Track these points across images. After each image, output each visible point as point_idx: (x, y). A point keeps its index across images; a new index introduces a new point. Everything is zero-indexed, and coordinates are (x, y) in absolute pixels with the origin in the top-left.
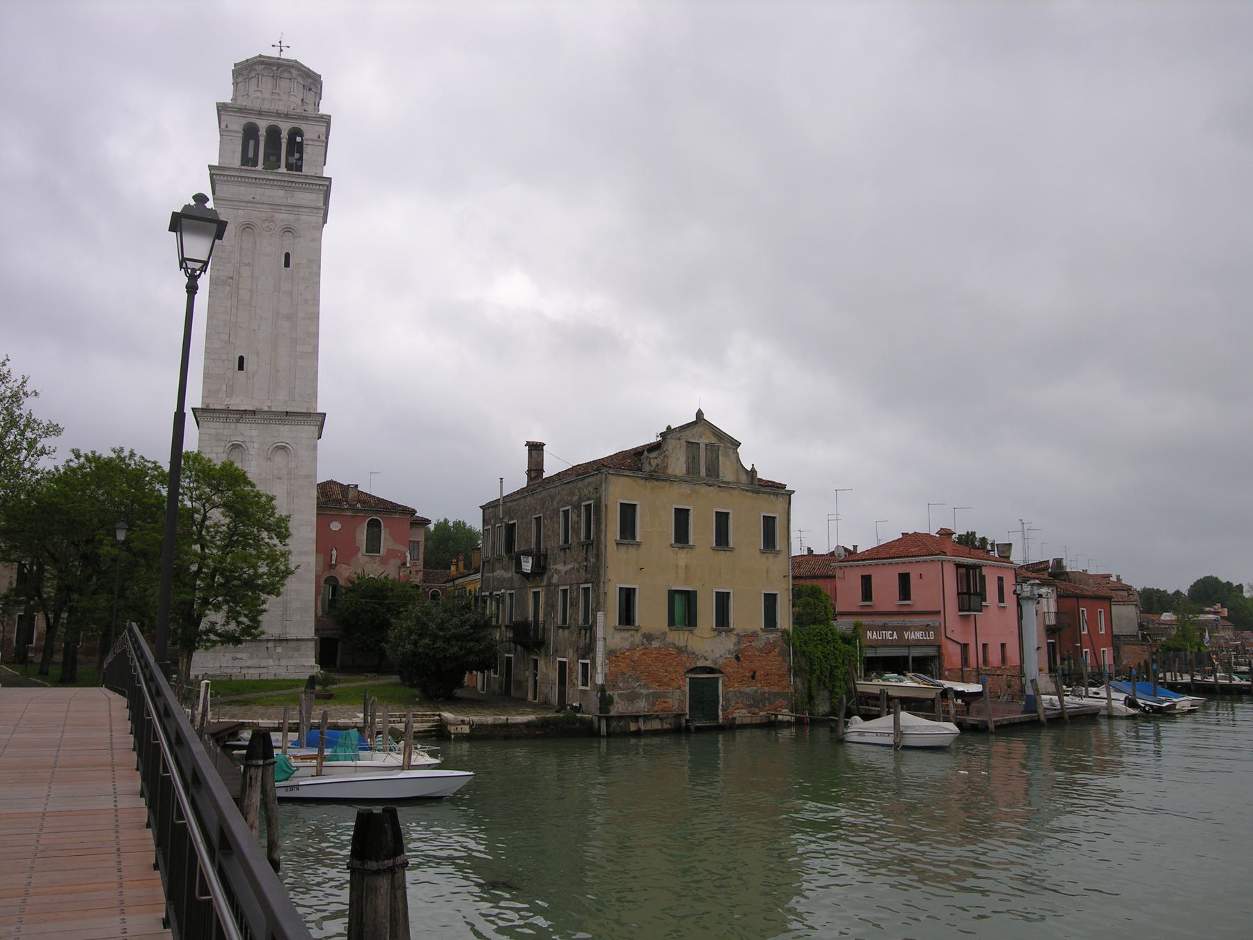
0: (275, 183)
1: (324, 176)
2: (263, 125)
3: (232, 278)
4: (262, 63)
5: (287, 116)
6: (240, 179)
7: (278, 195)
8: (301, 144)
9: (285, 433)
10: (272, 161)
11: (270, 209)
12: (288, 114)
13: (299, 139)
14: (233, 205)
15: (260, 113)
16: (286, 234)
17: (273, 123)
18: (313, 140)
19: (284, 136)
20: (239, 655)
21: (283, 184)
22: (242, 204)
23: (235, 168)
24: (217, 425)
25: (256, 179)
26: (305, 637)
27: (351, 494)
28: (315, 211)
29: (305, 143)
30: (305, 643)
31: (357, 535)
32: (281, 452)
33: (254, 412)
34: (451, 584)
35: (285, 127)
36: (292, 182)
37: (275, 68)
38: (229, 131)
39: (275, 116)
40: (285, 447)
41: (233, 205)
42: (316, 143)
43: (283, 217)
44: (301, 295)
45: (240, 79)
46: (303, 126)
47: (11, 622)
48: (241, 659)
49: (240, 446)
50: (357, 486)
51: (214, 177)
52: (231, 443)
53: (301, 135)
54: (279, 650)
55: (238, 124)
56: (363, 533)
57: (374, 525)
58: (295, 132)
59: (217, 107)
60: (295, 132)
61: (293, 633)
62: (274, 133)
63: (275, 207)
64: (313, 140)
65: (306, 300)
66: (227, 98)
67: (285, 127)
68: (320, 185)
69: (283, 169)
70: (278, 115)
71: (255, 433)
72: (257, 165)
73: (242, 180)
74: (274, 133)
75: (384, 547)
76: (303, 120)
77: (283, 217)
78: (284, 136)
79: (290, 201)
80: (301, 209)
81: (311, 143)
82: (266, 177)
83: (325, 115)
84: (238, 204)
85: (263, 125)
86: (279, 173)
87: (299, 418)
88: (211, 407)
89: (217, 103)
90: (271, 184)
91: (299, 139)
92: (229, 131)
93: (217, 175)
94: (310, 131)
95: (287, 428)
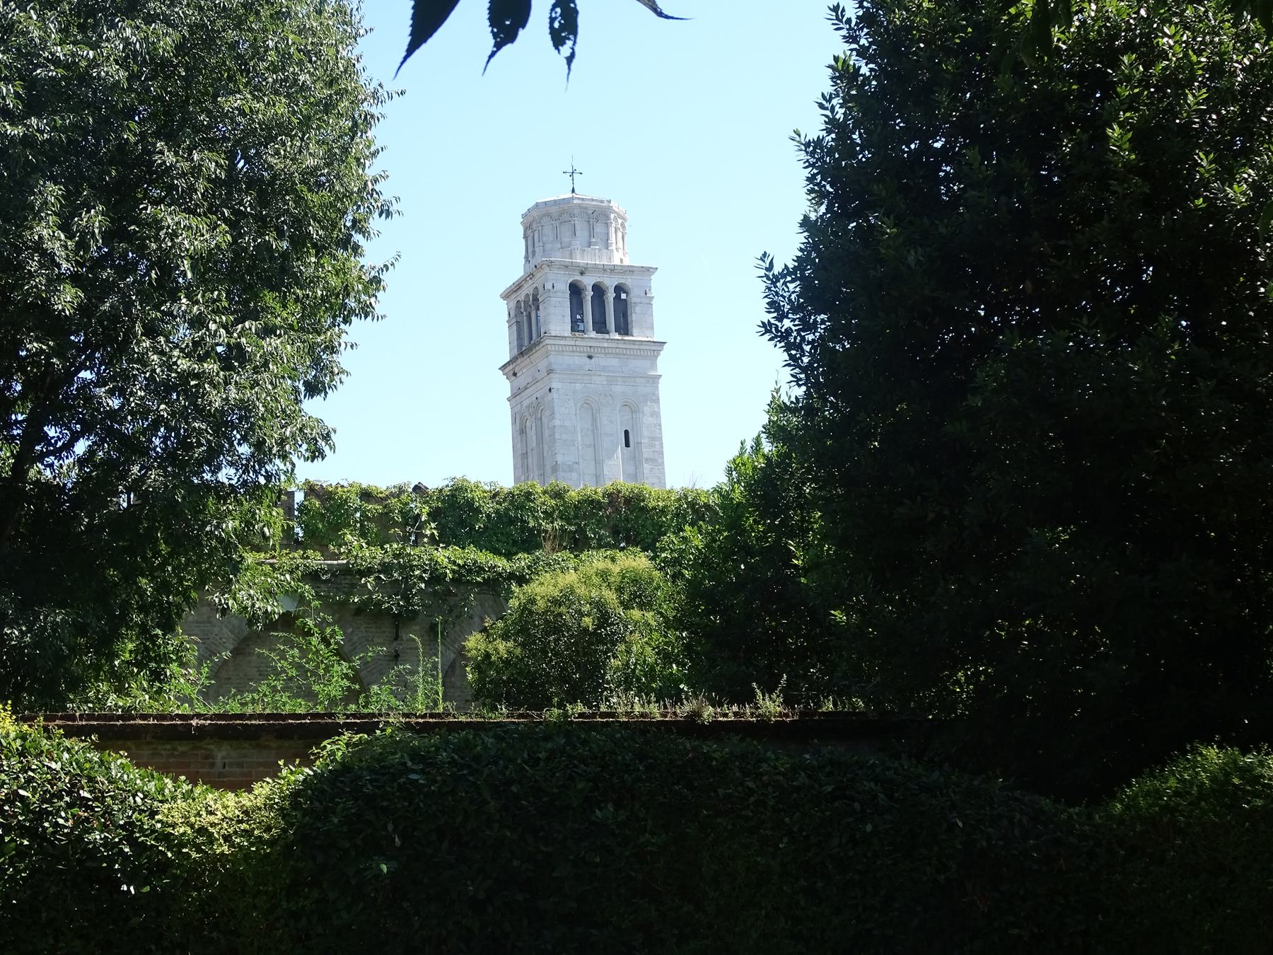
2: (588, 282)
3: (577, 463)
5: (613, 270)
19: (611, 295)
35: (610, 283)
38: (556, 292)
46: (628, 281)
58: (619, 289)
62: (599, 290)
70: (604, 269)
74: (599, 290)
78: (611, 295)
80: (638, 380)
85: (588, 282)
92: (556, 292)
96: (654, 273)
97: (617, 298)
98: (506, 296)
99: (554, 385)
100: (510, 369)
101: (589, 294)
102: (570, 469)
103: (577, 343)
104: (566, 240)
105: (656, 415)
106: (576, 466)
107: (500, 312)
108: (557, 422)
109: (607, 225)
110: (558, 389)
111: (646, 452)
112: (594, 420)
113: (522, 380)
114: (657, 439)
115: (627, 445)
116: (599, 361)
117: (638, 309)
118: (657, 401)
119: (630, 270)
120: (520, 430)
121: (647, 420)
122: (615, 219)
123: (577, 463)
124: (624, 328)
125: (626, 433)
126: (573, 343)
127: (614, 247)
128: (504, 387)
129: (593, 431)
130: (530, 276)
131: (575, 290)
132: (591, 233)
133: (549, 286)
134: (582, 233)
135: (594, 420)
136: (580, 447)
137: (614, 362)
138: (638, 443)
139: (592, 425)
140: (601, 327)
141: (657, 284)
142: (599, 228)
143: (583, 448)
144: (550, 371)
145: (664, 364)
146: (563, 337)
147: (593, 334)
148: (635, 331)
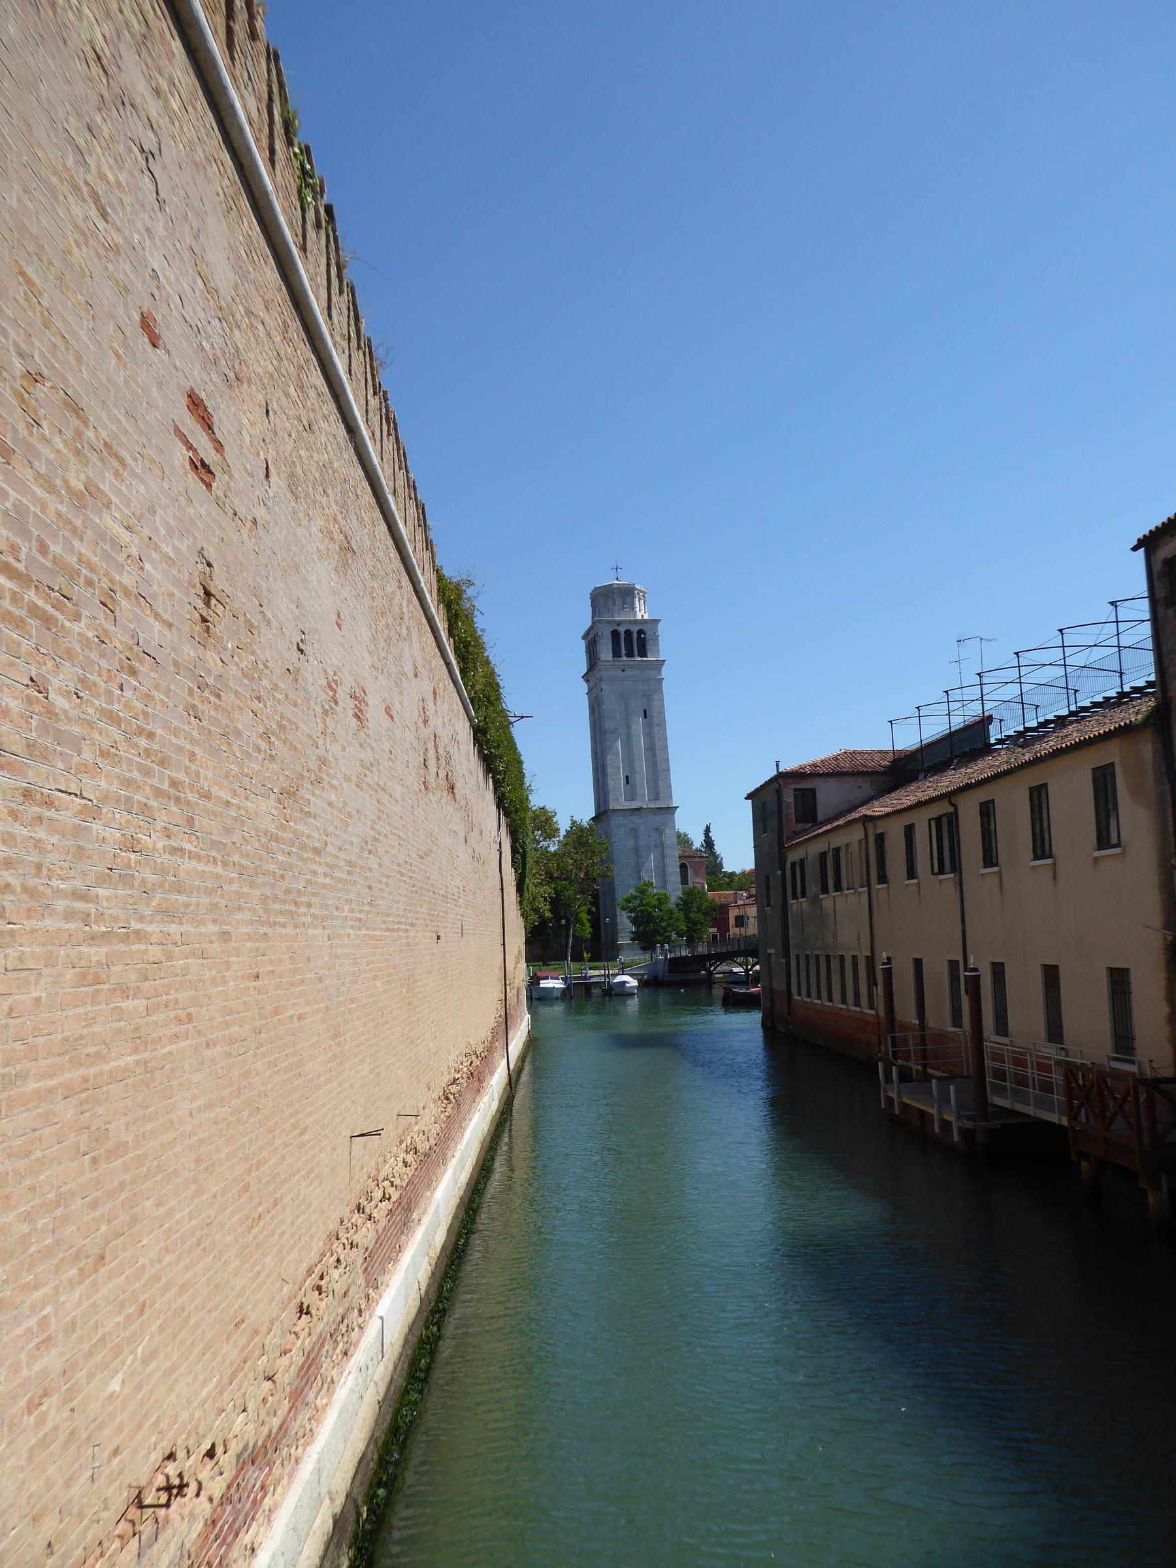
2: (622, 629)
5: (636, 622)
8: (644, 638)
9: (658, 819)
13: (643, 636)
19: (635, 636)
35: (635, 629)
46: (645, 627)
53: (644, 633)
58: (640, 632)
67: (635, 629)
71: (640, 821)
74: (628, 633)
78: (635, 636)
85: (622, 629)
91: (643, 636)
95: (657, 817)
97: (639, 637)
98: (584, 638)
99: (603, 687)
100: (586, 677)
101: (623, 636)
102: (613, 732)
104: (610, 607)
105: (662, 700)
107: (582, 646)
108: (605, 707)
109: (633, 597)
111: (656, 721)
112: (626, 704)
113: (591, 684)
114: (662, 713)
115: (645, 717)
116: (629, 672)
117: (650, 643)
118: (662, 692)
119: (646, 621)
120: (592, 711)
121: (656, 703)
122: (638, 594)
124: (643, 653)
125: (645, 711)
127: (637, 609)
128: (584, 687)
130: (592, 628)
131: (615, 634)
132: (624, 603)
133: (600, 634)
134: (619, 602)
135: (626, 704)
137: (636, 672)
140: (630, 654)
141: (661, 629)
142: (628, 599)
144: (601, 680)
145: (665, 672)
147: (625, 658)
148: (649, 655)
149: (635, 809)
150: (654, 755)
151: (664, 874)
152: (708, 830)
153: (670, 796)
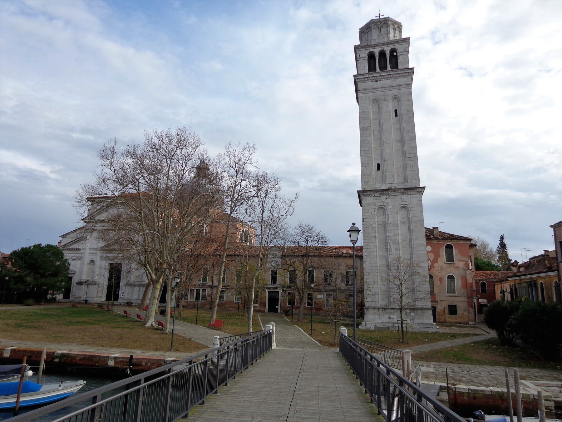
0: (386, 77)
1: (410, 67)
2: (377, 51)
3: (369, 126)
4: (373, 22)
5: (388, 43)
6: (369, 79)
7: (388, 82)
8: (396, 56)
9: (407, 199)
10: (383, 67)
11: (385, 90)
12: (388, 43)
13: (395, 54)
14: (367, 92)
15: (375, 46)
16: (395, 100)
17: (381, 49)
18: (402, 52)
20: (391, 316)
21: (390, 76)
22: (371, 90)
23: (366, 74)
24: (370, 198)
25: (376, 77)
26: (426, 307)
27: (435, 233)
28: (407, 86)
29: (398, 54)
30: (426, 311)
31: (440, 253)
32: (404, 209)
33: (387, 190)
34: (518, 278)
35: (387, 49)
36: (394, 74)
37: (379, 24)
38: (361, 58)
39: (382, 45)
40: (405, 206)
41: (367, 92)
42: (404, 53)
43: (391, 92)
44: (405, 129)
45: (363, 34)
46: (397, 46)
47: (285, 296)
48: (393, 318)
49: (382, 208)
50: (437, 228)
51: (357, 80)
52: (377, 207)
54: (413, 314)
55: (364, 54)
56: (443, 251)
57: (449, 247)
58: (393, 51)
59: (354, 48)
60: (393, 51)
61: (419, 305)
62: (382, 54)
63: (387, 88)
64: (402, 52)
65: (408, 131)
66: (358, 43)
67: (387, 49)
68: (408, 73)
69: (389, 69)
70: (384, 44)
72: (376, 70)
73: (369, 79)
74: (382, 54)
75: (455, 259)
76: (396, 43)
77: (391, 92)
79: (394, 84)
81: (401, 53)
82: (381, 75)
83: (407, 38)
84: (369, 91)
85: (377, 51)
86: (388, 71)
87: (411, 191)
88: (366, 189)
89: (354, 46)
90: (384, 77)
91: (395, 54)
92: (361, 58)
93: (357, 79)
94: (400, 48)
95: (404, 197)
96: (409, 40)
103: (370, 76)
106: (369, 128)
110: (361, 97)
111: (405, 117)
112: (379, 107)
123: (369, 126)
126: (367, 76)
129: (378, 113)
136: (372, 120)
138: (401, 114)
139: (378, 110)
143: (373, 120)
146: (362, 74)
149: (384, 190)
150: (403, 146)
151: (411, 246)
152: (502, 238)
153: (418, 179)
